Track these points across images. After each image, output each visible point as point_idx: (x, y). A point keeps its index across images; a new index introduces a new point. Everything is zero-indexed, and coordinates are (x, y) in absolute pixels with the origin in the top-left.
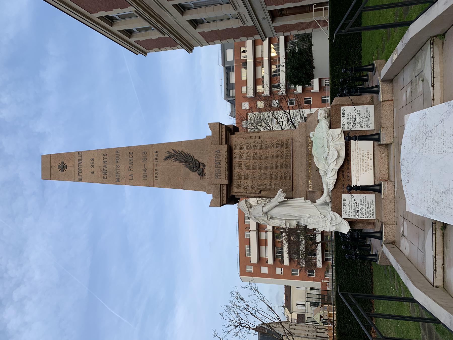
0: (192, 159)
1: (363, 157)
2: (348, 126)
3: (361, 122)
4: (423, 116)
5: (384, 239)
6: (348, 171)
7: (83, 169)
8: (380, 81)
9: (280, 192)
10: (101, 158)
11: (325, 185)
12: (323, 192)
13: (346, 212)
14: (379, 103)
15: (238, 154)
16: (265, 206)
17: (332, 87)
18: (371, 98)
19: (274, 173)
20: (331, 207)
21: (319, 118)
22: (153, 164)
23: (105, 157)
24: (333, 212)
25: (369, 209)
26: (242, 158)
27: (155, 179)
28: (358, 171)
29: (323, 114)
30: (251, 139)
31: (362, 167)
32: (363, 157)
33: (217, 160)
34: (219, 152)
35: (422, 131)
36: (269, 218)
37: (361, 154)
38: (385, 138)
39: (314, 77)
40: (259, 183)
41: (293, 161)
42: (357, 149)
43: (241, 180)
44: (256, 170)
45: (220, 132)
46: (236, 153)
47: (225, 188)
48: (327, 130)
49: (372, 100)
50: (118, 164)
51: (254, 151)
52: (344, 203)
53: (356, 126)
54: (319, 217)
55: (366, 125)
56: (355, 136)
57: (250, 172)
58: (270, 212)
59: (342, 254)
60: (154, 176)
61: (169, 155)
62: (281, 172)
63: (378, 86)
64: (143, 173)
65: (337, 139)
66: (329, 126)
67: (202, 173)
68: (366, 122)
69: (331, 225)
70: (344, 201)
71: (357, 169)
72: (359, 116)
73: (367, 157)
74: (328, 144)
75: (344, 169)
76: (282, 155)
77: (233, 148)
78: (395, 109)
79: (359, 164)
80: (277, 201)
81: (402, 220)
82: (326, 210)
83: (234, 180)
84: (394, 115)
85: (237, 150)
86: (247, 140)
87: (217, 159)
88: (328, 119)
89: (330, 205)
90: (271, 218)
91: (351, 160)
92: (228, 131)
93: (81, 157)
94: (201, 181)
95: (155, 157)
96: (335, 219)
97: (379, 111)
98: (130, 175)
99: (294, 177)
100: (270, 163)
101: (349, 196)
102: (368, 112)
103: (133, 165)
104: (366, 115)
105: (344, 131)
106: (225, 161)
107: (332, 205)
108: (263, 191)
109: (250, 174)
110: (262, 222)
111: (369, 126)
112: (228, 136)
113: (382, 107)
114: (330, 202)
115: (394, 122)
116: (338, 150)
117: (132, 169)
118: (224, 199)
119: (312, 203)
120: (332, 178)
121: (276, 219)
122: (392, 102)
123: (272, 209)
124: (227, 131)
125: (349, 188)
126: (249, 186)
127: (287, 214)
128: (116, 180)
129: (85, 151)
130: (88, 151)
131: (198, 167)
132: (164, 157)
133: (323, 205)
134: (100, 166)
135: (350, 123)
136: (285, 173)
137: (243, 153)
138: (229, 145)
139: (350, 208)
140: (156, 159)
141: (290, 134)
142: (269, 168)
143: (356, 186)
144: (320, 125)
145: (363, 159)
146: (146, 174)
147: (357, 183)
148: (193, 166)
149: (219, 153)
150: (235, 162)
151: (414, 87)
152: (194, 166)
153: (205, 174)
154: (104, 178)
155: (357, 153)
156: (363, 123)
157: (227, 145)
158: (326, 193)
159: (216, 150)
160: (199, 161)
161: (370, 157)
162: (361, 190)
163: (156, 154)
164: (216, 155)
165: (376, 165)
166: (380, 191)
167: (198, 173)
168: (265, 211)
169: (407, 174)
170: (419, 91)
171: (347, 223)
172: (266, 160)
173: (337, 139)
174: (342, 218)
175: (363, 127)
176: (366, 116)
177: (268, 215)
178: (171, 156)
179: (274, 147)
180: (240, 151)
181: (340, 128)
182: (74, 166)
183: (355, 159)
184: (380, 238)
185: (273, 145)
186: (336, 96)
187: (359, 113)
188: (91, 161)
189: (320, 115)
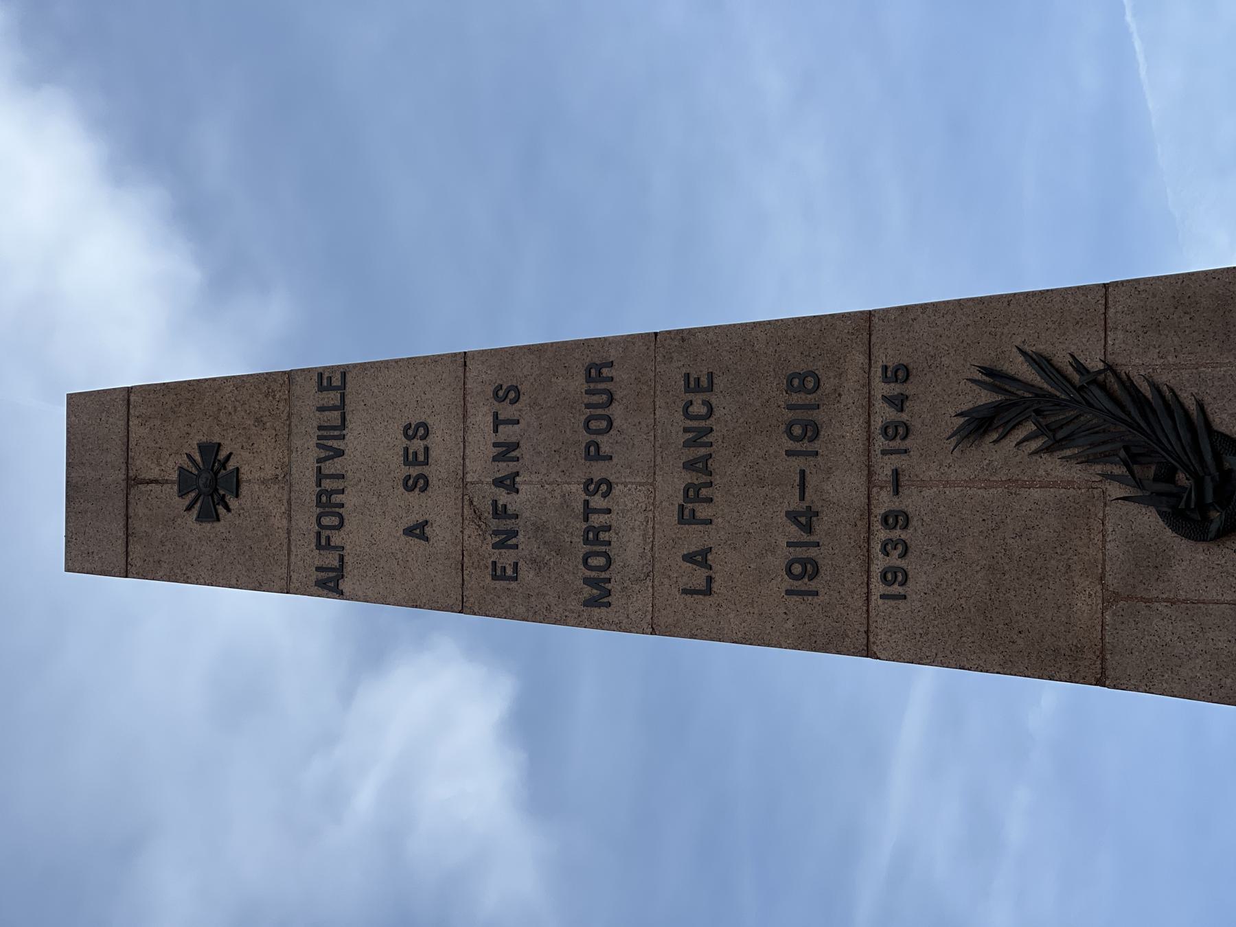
7: (350, 500)
10: (481, 418)
22: (870, 474)
23: (507, 411)
27: (883, 597)
50: (598, 470)
60: (873, 568)
61: (999, 398)
64: (789, 545)
93: (334, 408)
95: (883, 414)
98: (689, 558)
103: (717, 479)
117: (703, 511)
128: (587, 589)
129: (363, 366)
130: (386, 364)
132: (952, 412)
134: (469, 478)
140: (891, 431)
146: (813, 552)
152: (1209, 498)
154: (495, 577)
163: (894, 389)
178: (1015, 404)
182: (284, 478)
188: (406, 442)
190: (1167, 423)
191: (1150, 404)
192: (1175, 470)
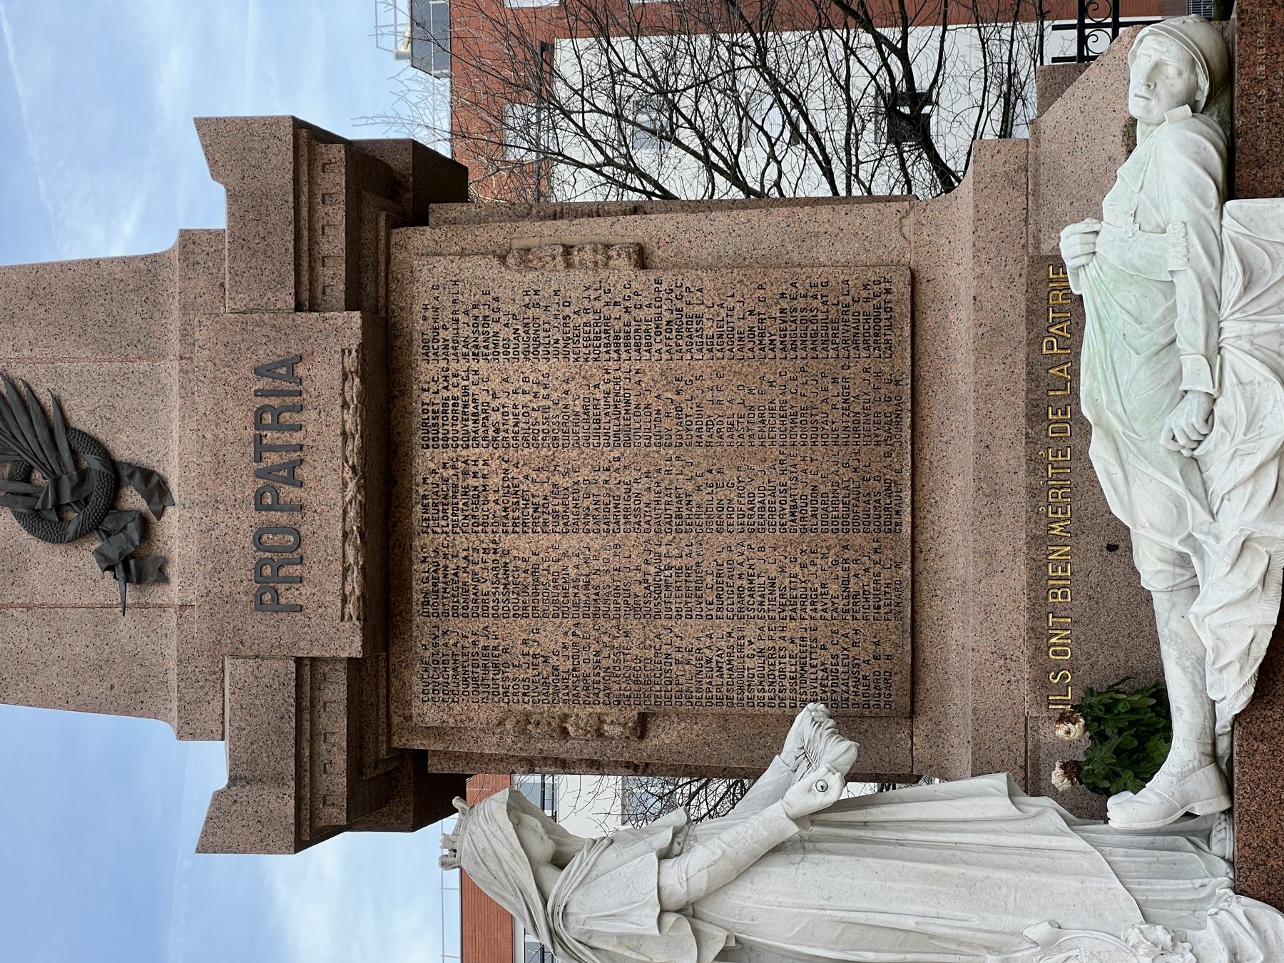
0: (43, 434)
11: (1184, 669)
15: (458, 392)
16: (677, 848)
19: (760, 566)
20: (1228, 854)
21: (1135, 108)
24: (1244, 899)
29: (1171, 71)
30: (569, 265)
33: (273, 448)
34: (292, 376)
43: (478, 625)
44: (611, 540)
46: (442, 384)
47: (336, 691)
51: (593, 369)
54: (1132, 941)
62: (824, 556)
66: (1220, 178)
74: (1214, 328)
76: (834, 407)
77: (411, 342)
83: (418, 619)
85: (443, 364)
86: (531, 275)
89: (1224, 841)
92: (368, 196)
96: (1261, 958)
100: (732, 475)
109: (553, 568)
112: (368, 236)
114: (1223, 812)
119: (1069, 823)
120: (1236, 614)
127: (862, 917)
136: (856, 561)
141: (895, 234)
149: (293, 387)
152: (67, 497)
157: (357, 314)
159: (264, 356)
160: (110, 445)
164: (266, 401)
167: (100, 554)
172: (699, 451)
177: (704, 927)
180: (474, 366)
185: (752, 321)
189: (1151, 83)
190: (23, 421)
192: (30, 470)
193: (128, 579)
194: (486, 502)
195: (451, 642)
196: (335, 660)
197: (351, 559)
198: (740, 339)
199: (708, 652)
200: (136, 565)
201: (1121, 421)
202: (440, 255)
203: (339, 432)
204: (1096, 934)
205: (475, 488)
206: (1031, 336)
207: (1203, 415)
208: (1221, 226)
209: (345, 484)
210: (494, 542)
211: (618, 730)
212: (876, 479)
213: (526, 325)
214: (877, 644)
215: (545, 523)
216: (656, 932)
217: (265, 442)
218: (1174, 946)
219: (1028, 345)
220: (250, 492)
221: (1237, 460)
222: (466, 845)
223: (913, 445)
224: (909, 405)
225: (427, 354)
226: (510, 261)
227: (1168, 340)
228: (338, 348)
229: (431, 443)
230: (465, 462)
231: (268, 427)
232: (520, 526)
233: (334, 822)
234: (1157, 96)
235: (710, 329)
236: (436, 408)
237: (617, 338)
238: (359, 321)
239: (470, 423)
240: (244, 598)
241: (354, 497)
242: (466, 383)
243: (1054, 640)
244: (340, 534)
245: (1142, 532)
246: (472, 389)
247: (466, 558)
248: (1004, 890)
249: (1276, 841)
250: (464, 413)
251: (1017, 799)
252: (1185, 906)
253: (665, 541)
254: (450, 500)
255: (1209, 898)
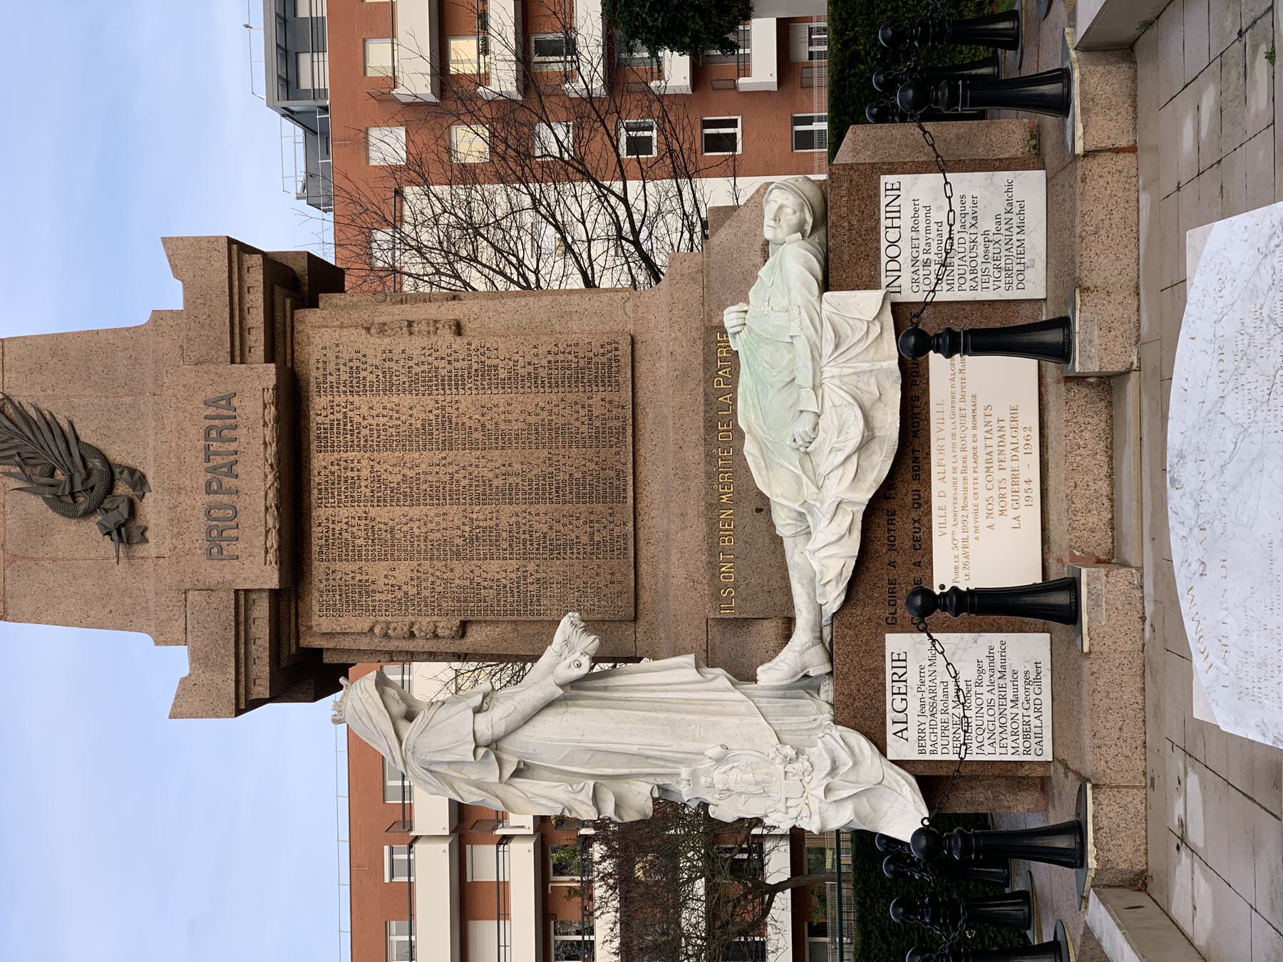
0: (62, 446)
1: (989, 442)
2: (916, 277)
3: (980, 259)
4: (1271, 238)
5: (1092, 862)
6: (914, 515)
8: (1076, 49)
9: (569, 629)
11: (802, 585)
12: (790, 622)
13: (905, 726)
14: (1068, 160)
15: (340, 416)
16: (485, 706)
17: (842, 71)
18: (1032, 137)
19: (536, 526)
20: (831, 700)
21: (768, 234)
24: (840, 727)
25: (1020, 711)
26: (362, 443)
28: (965, 513)
29: (789, 211)
30: (411, 333)
31: (984, 494)
32: (989, 442)
33: (216, 453)
34: (229, 405)
35: (1266, 311)
36: (510, 769)
37: (980, 420)
38: (1096, 341)
39: (751, 9)
40: (457, 581)
41: (641, 460)
42: (958, 397)
43: (355, 566)
44: (441, 510)
45: (236, 290)
47: (261, 611)
48: (809, 296)
49: (1034, 147)
51: (429, 401)
52: (896, 678)
53: (956, 277)
54: (772, 755)
55: (1003, 273)
56: (949, 330)
57: (404, 520)
58: (513, 737)
59: (888, 944)
62: (578, 518)
63: (1063, 76)
65: (863, 346)
66: (820, 278)
67: (123, 525)
68: (1003, 259)
69: (832, 798)
70: (895, 670)
71: (960, 502)
72: (968, 225)
73: (1008, 439)
74: (817, 371)
75: (893, 504)
76: (583, 423)
77: (308, 383)
78: (1145, 198)
79: (970, 475)
80: (551, 680)
81: (1176, 762)
82: (806, 719)
83: (316, 563)
84: (1138, 224)
85: (330, 398)
86: (387, 340)
87: (215, 446)
88: (816, 238)
90: (517, 773)
91: (929, 454)
92: (277, 288)
94: (121, 570)
96: (851, 763)
97: (1068, 205)
99: (642, 544)
101: (921, 642)
102: (1016, 209)
104: (1003, 222)
105: (895, 306)
106: (262, 456)
107: (835, 690)
108: (479, 622)
109: (405, 528)
110: (475, 794)
111: (1021, 282)
112: (278, 313)
113: (1082, 181)
114: (827, 674)
115: (1138, 264)
116: (867, 404)
118: (254, 671)
119: (733, 684)
120: (834, 550)
121: (546, 774)
122: (1130, 158)
123: (527, 720)
124: (272, 291)
125: (918, 601)
126: (400, 594)
127: (603, 746)
131: (100, 489)
133: (789, 693)
135: (926, 264)
136: (598, 522)
137: (364, 411)
138: (289, 365)
139: (927, 707)
141: (621, 312)
142: (508, 494)
143: (954, 589)
144: (773, 268)
145: (989, 450)
147: (962, 573)
148: (72, 486)
149: (231, 413)
150: (320, 461)
151: (1231, 89)
152: (78, 487)
153: (142, 534)
155: (957, 419)
156: (990, 266)
157: (273, 365)
158: (808, 628)
159: (210, 393)
160: (107, 453)
161: (1022, 442)
162: (978, 613)
164: (212, 422)
165: (1052, 483)
166: (1070, 616)
168: (485, 732)
169: (1196, 529)
170: (1253, 111)
171: (910, 784)
172: (497, 452)
173: (863, 346)
174: (883, 759)
175: (990, 285)
176: (1007, 226)
177: (504, 756)
179: (534, 380)
180: (350, 398)
181: (877, 286)
183: (948, 452)
184: (1075, 859)
186: (859, 119)
187: (969, 210)
189: (776, 219)
191: (35, 422)
192: (54, 469)
193: (121, 540)
194: (360, 487)
195: (338, 578)
196: (260, 590)
197: (270, 524)
198: (522, 381)
199: (504, 581)
200: (126, 532)
201: (762, 429)
202: (327, 327)
203: (262, 442)
204: (749, 752)
205: (352, 478)
206: (707, 377)
207: (812, 425)
208: (821, 308)
209: (266, 476)
210: (365, 512)
211: (447, 632)
212: (611, 469)
213: (384, 372)
214: (612, 574)
215: (398, 500)
216: (473, 760)
217: (211, 449)
218: (797, 758)
219: (705, 383)
220: (202, 483)
221: (833, 454)
222: (348, 707)
223: (634, 447)
224: (631, 421)
225: (319, 392)
226: (373, 331)
227: (788, 380)
228: (260, 388)
229: (323, 449)
230: (346, 461)
231: (213, 439)
232: (382, 502)
233: (261, 696)
234: (781, 227)
235: (503, 374)
236: (325, 426)
237: (443, 380)
238: (274, 370)
239: (349, 436)
240: (199, 552)
241: (273, 484)
242: (345, 410)
243: (723, 569)
244: (263, 509)
245: (776, 500)
246: (350, 414)
247: (347, 523)
248: (693, 727)
249: (859, 690)
250: (345, 429)
251: (700, 670)
252: (804, 733)
253: (476, 510)
254: (336, 486)
255: (819, 727)
